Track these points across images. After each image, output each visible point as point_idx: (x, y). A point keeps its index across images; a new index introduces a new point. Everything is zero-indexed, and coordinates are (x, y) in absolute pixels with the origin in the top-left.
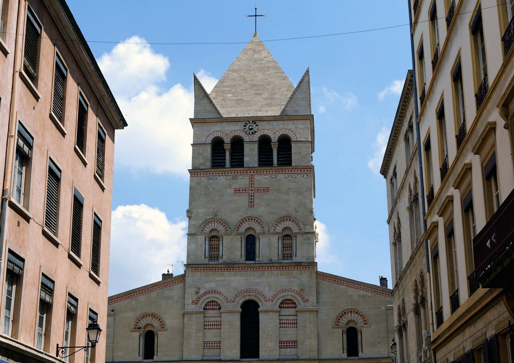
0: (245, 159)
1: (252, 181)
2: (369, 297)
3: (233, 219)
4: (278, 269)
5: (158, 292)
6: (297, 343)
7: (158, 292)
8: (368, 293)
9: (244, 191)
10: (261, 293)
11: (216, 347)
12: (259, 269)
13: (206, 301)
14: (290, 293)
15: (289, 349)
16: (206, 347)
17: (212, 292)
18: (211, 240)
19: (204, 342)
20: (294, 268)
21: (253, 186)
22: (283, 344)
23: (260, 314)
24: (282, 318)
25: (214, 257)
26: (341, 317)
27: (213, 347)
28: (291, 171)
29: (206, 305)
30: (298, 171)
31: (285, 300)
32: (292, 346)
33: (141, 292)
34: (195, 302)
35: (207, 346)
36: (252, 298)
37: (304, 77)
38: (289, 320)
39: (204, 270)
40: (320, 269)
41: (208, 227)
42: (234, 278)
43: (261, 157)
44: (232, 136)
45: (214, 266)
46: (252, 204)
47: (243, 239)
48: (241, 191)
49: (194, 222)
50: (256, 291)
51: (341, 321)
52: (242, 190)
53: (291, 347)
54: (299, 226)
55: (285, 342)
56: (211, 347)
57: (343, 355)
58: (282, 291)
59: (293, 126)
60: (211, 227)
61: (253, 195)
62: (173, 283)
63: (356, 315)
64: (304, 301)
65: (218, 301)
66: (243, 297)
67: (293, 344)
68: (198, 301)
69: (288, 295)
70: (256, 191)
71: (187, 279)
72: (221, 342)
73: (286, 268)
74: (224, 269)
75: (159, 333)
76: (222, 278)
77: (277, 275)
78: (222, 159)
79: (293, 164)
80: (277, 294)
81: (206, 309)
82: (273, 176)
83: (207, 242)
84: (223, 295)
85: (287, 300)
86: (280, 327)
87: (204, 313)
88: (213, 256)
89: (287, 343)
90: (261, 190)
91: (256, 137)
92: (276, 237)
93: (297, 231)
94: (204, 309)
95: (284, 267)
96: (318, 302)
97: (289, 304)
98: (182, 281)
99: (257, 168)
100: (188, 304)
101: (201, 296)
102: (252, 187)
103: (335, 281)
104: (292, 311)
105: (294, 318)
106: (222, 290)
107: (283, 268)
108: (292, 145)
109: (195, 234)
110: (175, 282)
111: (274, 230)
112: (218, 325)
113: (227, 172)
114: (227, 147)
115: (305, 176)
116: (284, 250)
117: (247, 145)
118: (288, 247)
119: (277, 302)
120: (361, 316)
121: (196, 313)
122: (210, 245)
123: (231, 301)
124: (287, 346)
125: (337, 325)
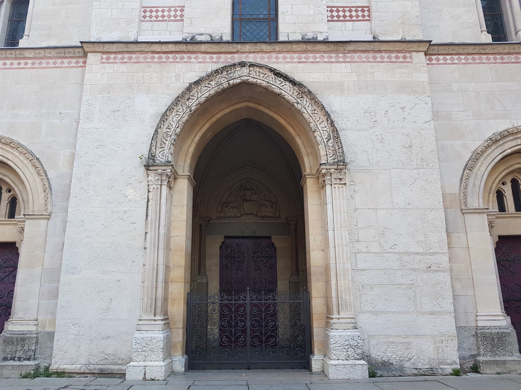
6: (369, 11)
11: (172, 18)
16: (148, 19)
19: (143, 7)
27: (166, 18)
35: (151, 17)
53: (354, 18)
55: (341, 9)
56: (160, 18)
67: (360, 13)
72: (184, 7)
124: (344, 16)
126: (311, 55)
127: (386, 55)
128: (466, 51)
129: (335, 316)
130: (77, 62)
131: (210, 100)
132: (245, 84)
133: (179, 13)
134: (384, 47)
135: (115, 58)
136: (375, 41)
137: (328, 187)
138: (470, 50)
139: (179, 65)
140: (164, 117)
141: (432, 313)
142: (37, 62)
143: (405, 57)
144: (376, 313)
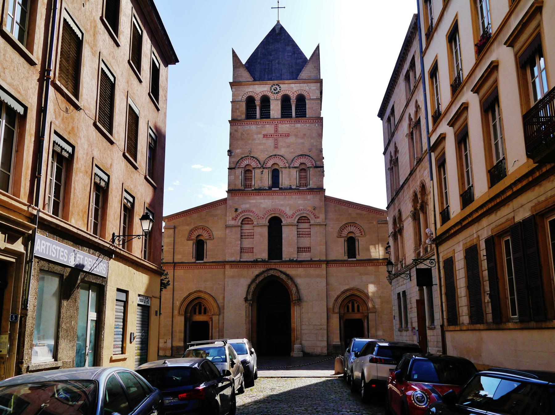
0: (271, 113)
1: (276, 129)
2: (365, 215)
3: (262, 157)
4: (296, 194)
5: (206, 211)
7: (206, 211)
8: (363, 212)
9: (270, 136)
10: (283, 212)
12: (282, 194)
13: (242, 218)
14: (305, 212)
15: (304, 253)
17: (247, 211)
18: (246, 172)
20: (308, 193)
21: (277, 132)
22: (300, 250)
23: (283, 227)
24: (299, 230)
25: (248, 186)
26: (343, 229)
28: (306, 121)
29: (242, 221)
30: (311, 121)
31: (302, 217)
32: (307, 251)
33: (194, 211)
34: (234, 219)
35: (243, 251)
36: (277, 215)
37: (315, 51)
38: (304, 232)
39: (241, 195)
40: (327, 194)
41: (243, 163)
42: (262, 201)
43: (283, 111)
44: (261, 95)
45: (248, 192)
46: (277, 146)
47: (270, 172)
48: (268, 136)
49: (233, 160)
50: (279, 210)
51: (344, 232)
52: (269, 136)
54: (312, 162)
57: (345, 257)
58: (300, 210)
59: (307, 88)
60: (246, 163)
61: (277, 139)
62: (217, 205)
63: (354, 228)
64: (316, 218)
65: (251, 218)
66: (270, 215)
67: (308, 249)
68: (236, 218)
69: (303, 213)
70: (280, 136)
71: (228, 201)
73: (302, 194)
74: (256, 194)
75: (208, 241)
76: (254, 201)
77: (296, 199)
78: (254, 113)
79: (307, 116)
80: (296, 212)
81: (243, 224)
82: (292, 125)
83: (243, 174)
84: (255, 213)
85: (303, 217)
86: (298, 237)
87: (241, 227)
88: (247, 185)
89: (303, 249)
90: (283, 135)
91: (279, 96)
92: (295, 170)
93: (310, 166)
94: (241, 223)
95: (301, 193)
96: (326, 219)
97: (304, 220)
98: (225, 203)
99: (280, 119)
100: (229, 220)
101: (239, 214)
102: (276, 133)
103: (339, 203)
104: (306, 225)
105: (308, 230)
106: (254, 210)
107: (300, 194)
108: (307, 102)
109: (234, 168)
110: (219, 204)
111: (293, 165)
112: (252, 235)
113: (257, 122)
114: (258, 103)
115: (316, 125)
116: (300, 180)
117: (273, 102)
118: (303, 178)
119: (295, 218)
120: (358, 229)
121: (235, 226)
122: (245, 177)
123: (261, 218)
124: (303, 251)
125: (340, 236)
126: (292, 265)
127: (314, 265)
128: (339, 263)
129: (296, 341)
130: (222, 267)
131: (262, 280)
132: (272, 275)
133: (252, 250)
134: (314, 263)
135: (234, 267)
136: (311, 261)
137: (295, 307)
138: (340, 262)
139: (253, 269)
140: (249, 286)
141: (321, 341)
142: (210, 266)
143: (320, 266)
144: (306, 341)
